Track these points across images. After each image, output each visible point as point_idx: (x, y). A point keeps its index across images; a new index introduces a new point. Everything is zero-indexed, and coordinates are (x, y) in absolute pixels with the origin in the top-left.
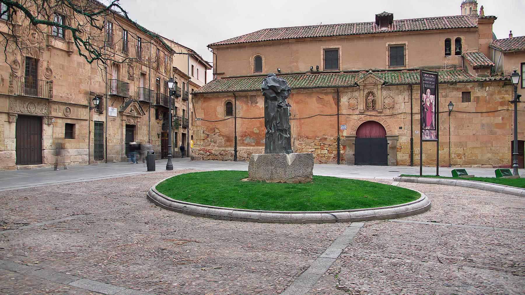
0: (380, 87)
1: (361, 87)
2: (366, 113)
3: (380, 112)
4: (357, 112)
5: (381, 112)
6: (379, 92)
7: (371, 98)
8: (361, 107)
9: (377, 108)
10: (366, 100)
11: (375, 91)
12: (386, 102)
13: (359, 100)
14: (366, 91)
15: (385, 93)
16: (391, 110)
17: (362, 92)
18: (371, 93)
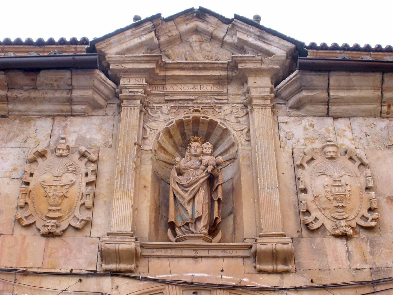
0: (260, 86)
1: (132, 84)
2: (159, 268)
3: (274, 256)
4: (82, 254)
5: (283, 259)
6: (260, 118)
7: (199, 157)
8: (122, 213)
9: (247, 228)
10: (161, 183)
11: (228, 116)
12: (318, 183)
13: (105, 168)
14: (163, 119)
15: (301, 131)
16: (359, 245)
17: (131, 116)
18: (194, 130)
